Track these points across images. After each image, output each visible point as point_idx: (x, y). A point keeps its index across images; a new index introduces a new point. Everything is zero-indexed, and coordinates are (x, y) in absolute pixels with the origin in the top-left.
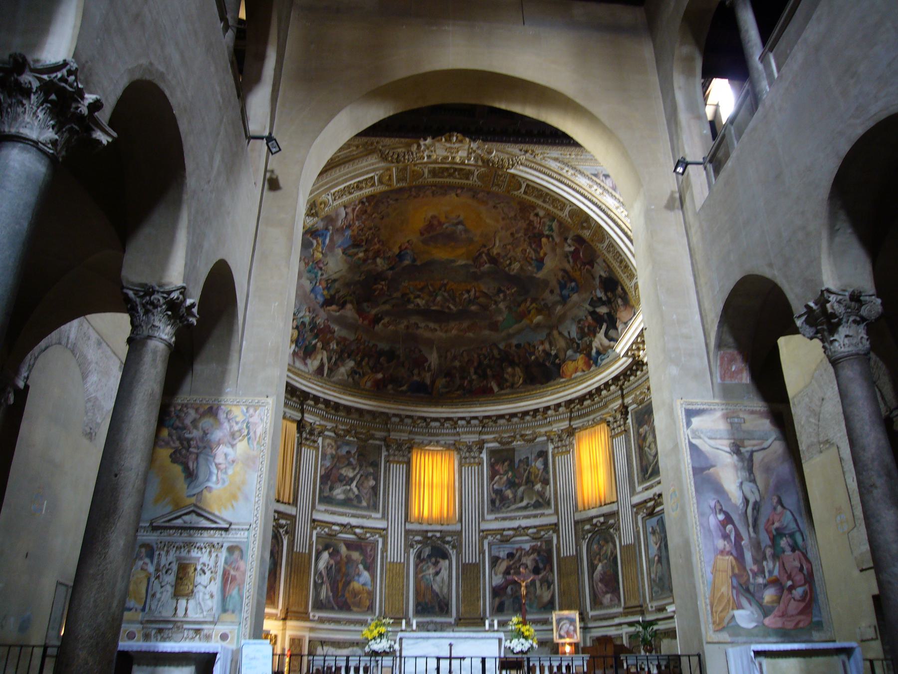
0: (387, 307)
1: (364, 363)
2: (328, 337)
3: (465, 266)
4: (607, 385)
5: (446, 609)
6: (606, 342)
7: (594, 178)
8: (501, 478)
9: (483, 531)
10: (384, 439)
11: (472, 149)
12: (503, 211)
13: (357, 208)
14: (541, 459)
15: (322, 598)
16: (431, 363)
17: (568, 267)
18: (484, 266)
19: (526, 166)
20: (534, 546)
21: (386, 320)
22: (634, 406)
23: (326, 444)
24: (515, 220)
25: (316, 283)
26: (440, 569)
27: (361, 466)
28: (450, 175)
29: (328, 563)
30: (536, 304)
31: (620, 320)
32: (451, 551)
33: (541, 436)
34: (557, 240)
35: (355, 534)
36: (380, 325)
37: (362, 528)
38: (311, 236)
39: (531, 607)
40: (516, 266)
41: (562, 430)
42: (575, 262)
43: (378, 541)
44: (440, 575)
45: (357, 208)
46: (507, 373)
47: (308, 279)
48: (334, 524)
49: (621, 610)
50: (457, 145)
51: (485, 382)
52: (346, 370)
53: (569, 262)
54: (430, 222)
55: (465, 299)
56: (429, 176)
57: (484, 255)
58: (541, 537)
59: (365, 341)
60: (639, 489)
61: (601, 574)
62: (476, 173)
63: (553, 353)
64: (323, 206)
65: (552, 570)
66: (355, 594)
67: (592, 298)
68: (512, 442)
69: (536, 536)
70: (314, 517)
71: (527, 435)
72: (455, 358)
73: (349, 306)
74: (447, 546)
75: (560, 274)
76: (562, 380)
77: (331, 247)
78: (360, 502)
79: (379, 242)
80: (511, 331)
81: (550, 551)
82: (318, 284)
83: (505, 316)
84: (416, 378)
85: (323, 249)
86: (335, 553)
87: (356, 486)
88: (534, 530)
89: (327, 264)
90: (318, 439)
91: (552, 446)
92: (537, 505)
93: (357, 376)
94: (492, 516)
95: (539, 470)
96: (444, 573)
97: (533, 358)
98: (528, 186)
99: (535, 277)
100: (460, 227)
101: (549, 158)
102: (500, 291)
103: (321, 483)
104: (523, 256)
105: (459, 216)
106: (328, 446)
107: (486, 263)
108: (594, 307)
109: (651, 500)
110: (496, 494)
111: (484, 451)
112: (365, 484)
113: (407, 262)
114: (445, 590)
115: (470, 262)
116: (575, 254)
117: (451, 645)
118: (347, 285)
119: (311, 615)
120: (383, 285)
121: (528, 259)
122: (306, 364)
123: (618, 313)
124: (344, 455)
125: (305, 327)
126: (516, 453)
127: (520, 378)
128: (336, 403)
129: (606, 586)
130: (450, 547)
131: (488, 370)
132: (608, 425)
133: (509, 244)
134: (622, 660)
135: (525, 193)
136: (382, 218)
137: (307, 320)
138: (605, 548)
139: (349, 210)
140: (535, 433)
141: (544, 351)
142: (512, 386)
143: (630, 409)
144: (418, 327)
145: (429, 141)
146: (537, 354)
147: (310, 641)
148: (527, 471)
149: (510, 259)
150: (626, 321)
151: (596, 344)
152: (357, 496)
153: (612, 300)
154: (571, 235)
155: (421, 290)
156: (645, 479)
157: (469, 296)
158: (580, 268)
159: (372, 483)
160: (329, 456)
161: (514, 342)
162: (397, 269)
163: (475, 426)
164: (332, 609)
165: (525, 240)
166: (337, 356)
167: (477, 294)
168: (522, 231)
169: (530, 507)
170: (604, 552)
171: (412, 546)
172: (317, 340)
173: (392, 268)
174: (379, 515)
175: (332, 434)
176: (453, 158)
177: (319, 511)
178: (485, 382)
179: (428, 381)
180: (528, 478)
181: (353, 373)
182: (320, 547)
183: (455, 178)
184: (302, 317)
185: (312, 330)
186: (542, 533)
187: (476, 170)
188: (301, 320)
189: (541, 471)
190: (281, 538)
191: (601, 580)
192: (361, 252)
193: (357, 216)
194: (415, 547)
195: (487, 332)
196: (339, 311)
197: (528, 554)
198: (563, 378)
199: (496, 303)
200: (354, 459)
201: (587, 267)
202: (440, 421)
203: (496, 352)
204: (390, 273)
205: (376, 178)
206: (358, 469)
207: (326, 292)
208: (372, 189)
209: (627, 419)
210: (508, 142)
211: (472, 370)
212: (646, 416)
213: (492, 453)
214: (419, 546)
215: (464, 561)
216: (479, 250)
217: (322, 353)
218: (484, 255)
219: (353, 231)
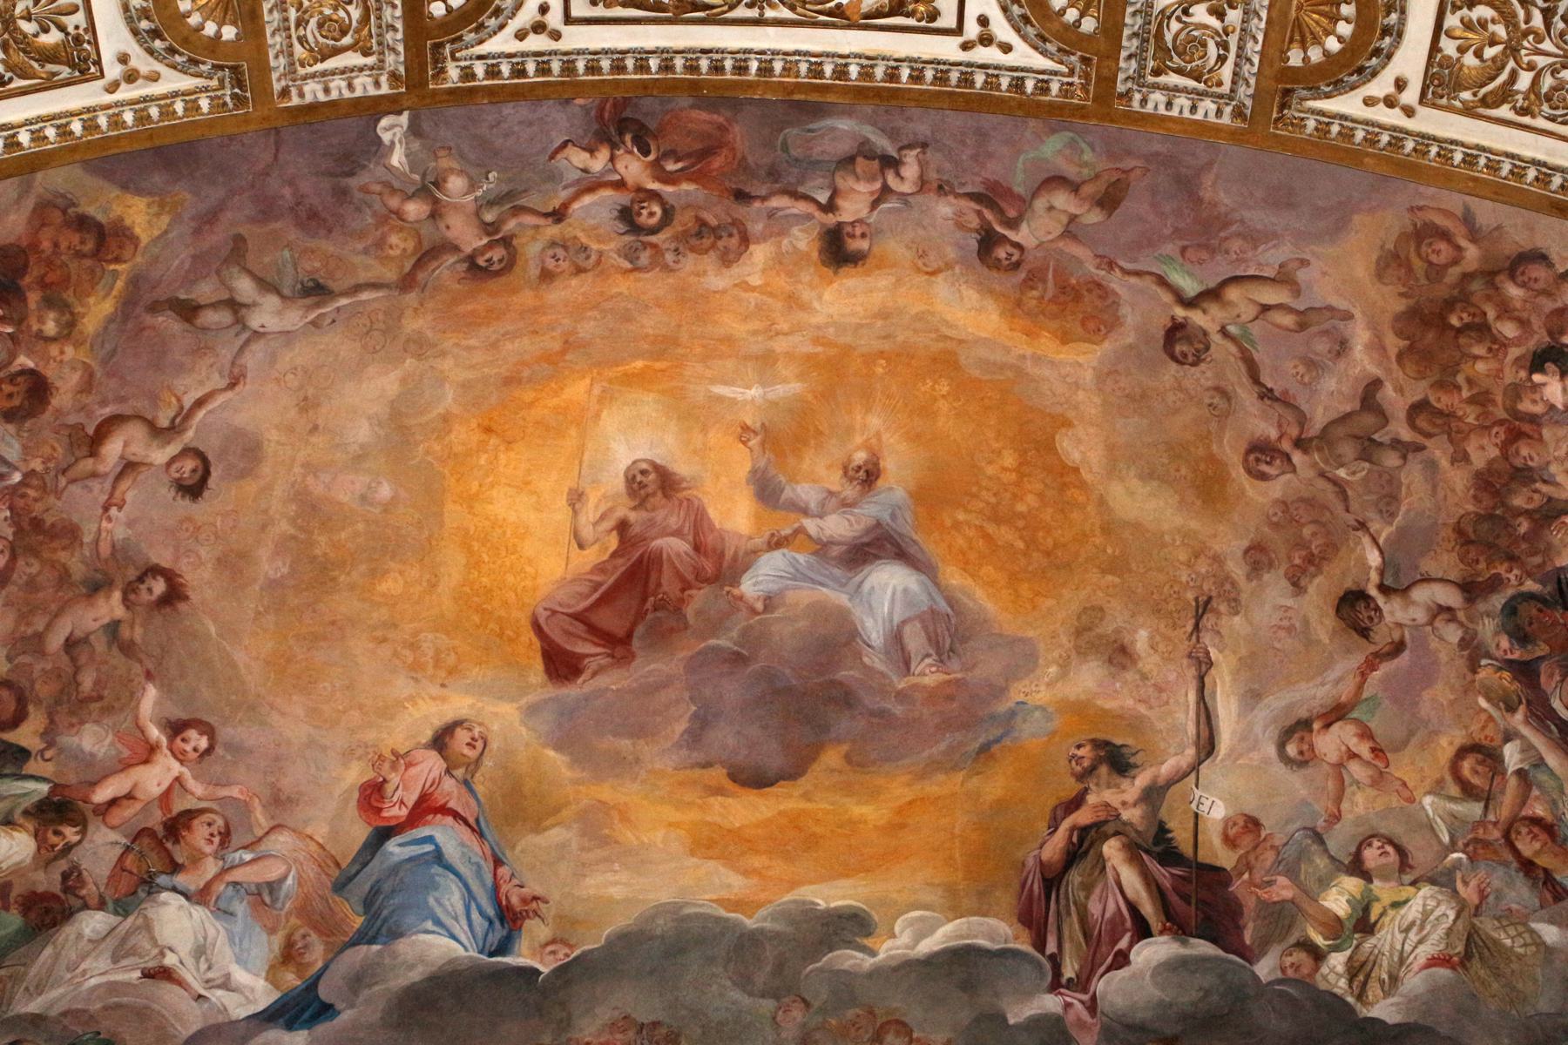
12: (1255, 378)
18: (1122, 960)
24: (1368, 448)
54: (622, 527)
57: (1112, 850)
79: (176, 729)
104: (1476, 809)
105: (869, 476)
107: (1143, 931)
121: (1527, 847)
133: (1336, 713)
136: (194, 489)
149: (1357, 867)
162: (346, 1016)
165: (1473, 651)
168: (1446, 562)
216: (1076, 803)
218: (1112, 850)
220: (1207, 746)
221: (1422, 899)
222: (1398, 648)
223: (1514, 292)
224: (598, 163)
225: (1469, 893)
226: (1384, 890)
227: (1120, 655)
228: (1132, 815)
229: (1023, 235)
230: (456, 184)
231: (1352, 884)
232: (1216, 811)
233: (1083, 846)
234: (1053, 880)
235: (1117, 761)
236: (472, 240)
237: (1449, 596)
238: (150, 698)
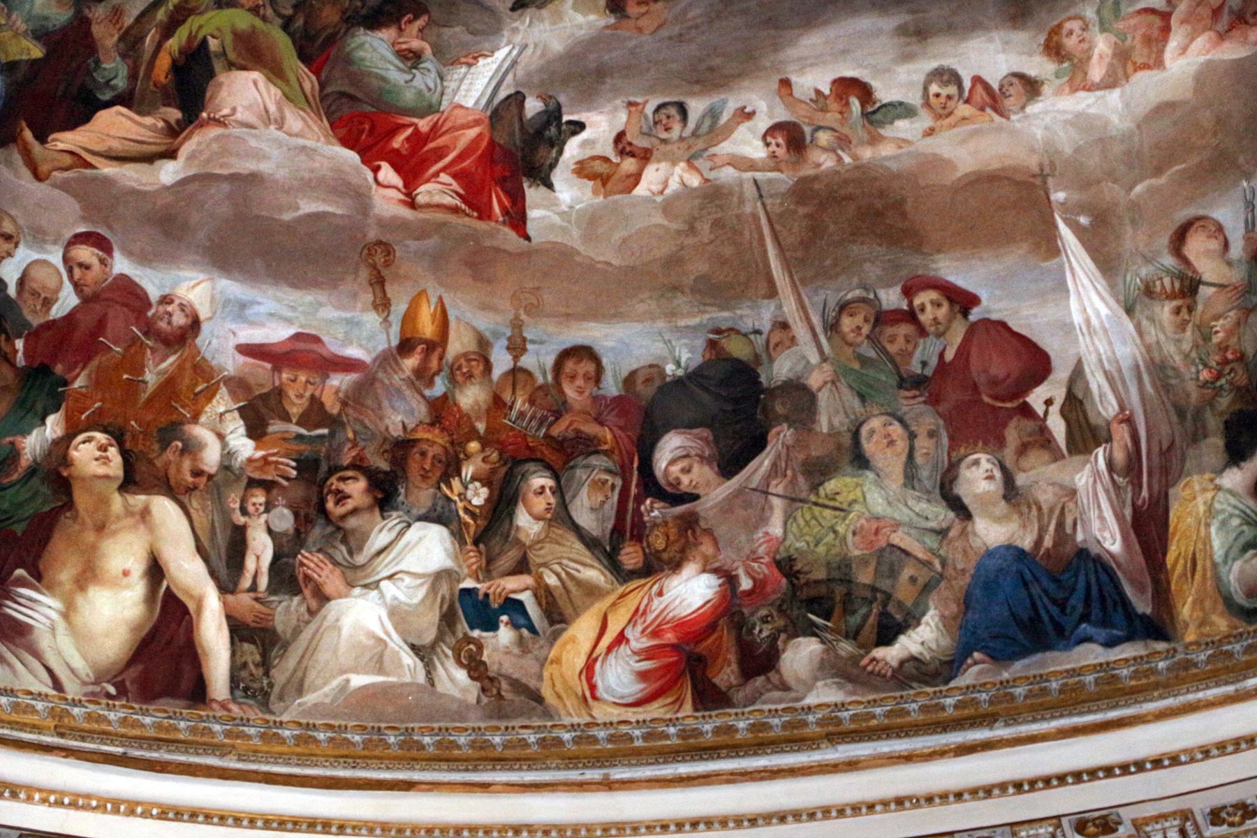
1: (526, 523)
2: (151, 377)
16: (1078, 373)
36: (560, 177)
52: (397, 614)
59: (483, 344)
166: (284, 519)
172: (53, 426)
196: (171, 154)
217: (145, 514)
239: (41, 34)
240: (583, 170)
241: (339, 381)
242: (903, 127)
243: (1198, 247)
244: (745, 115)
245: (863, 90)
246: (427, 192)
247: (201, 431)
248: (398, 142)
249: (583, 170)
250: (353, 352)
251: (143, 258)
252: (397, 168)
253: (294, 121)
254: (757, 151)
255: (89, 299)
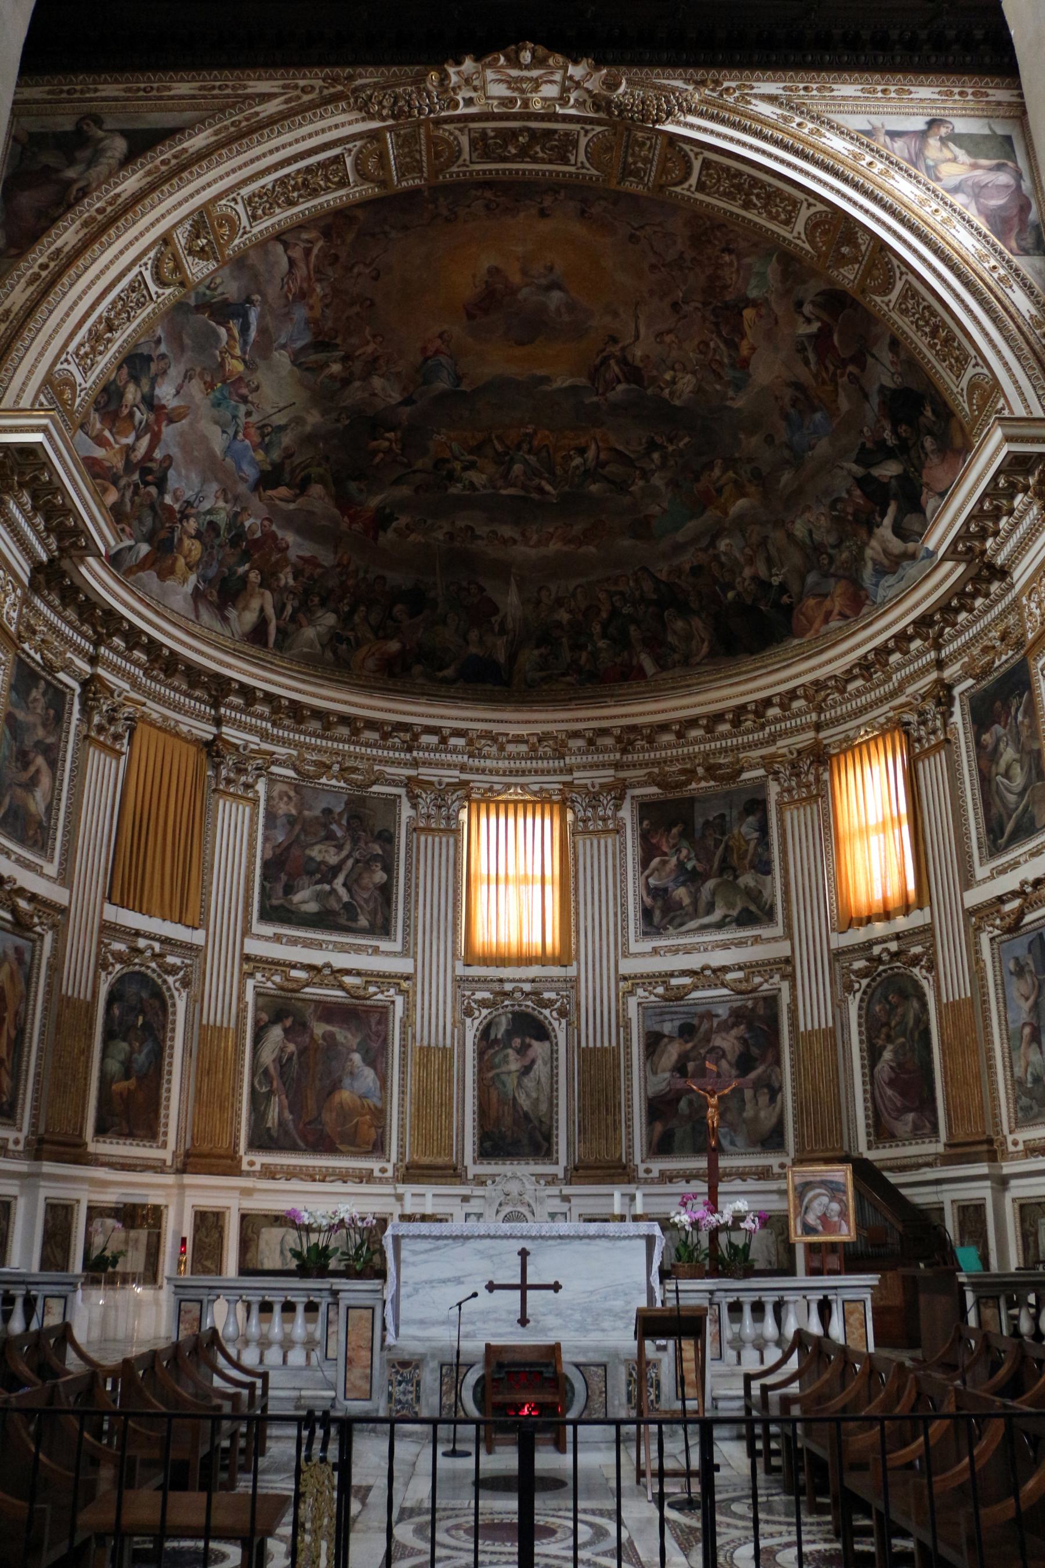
0: (405, 491)
1: (357, 619)
2: (273, 559)
3: (573, 388)
4: (902, 639)
5: (545, 1145)
6: (896, 545)
7: (865, 140)
8: (664, 863)
9: (625, 978)
10: (410, 783)
11: (571, 78)
13: (315, 251)
14: (751, 819)
15: (269, 1124)
16: (505, 616)
17: (804, 374)
18: (614, 389)
19: (701, 115)
20: (739, 1008)
21: (403, 520)
22: (970, 682)
23: (275, 794)
25: (236, 433)
26: (533, 1062)
27: (355, 841)
28: (524, 153)
29: (282, 1050)
30: (735, 473)
31: (931, 490)
32: (556, 1024)
33: (753, 767)
34: (779, 309)
35: (341, 987)
37: (358, 973)
38: (210, 316)
39: (733, 1143)
40: (687, 383)
41: (799, 752)
42: (821, 361)
43: (393, 1002)
44: (532, 1074)
45: (315, 251)
46: (675, 632)
47: (217, 423)
48: (294, 966)
49: (940, 1148)
50: (535, 73)
51: (626, 654)
52: (319, 635)
53: (807, 363)
55: (577, 467)
56: (475, 155)
57: (612, 362)
58: (754, 990)
60: (981, 872)
61: (891, 1067)
62: (583, 141)
63: (776, 581)
64: (225, 230)
65: (778, 1061)
66: (345, 1113)
67: (863, 444)
68: (688, 782)
69: (744, 986)
70: (246, 951)
71: (720, 766)
72: (559, 602)
73: (317, 489)
74: (546, 1012)
75: (789, 393)
76: (796, 642)
77: (265, 345)
78: (354, 918)
79: (374, 336)
80: (680, 537)
81: (773, 1021)
82: (240, 436)
83: (665, 505)
84: (473, 650)
85: (244, 352)
86: (298, 1029)
87: (345, 885)
88: (740, 975)
89: (257, 388)
90: (256, 782)
91: (778, 789)
92: (746, 919)
93: (344, 646)
94: (647, 945)
95: (747, 842)
96: (540, 1069)
97: (730, 595)
98: (706, 164)
99: (730, 408)
100: (556, 295)
101: (756, 96)
102: (652, 446)
103: (265, 877)
105: (551, 269)
106: (281, 799)
107: (619, 382)
108: (868, 465)
109: (1014, 894)
110: (654, 898)
111: (627, 805)
112: (365, 881)
113: (443, 384)
114: (544, 1107)
115: (583, 381)
116: (821, 341)
117: (524, 1254)
118: (308, 440)
119: (245, 1160)
120: (388, 440)
121: (714, 367)
122: (225, 619)
123: (925, 472)
124: (317, 818)
125: (218, 535)
126: (697, 806)
127: (703, 641)
128: (292, 701)
129: (903, 1094)
130: (555, 1014)
131: (632, 628)
132: (907, 733)
134: (963, 1284)
135: (701, 187)
136: (376, 278)
137: (221, 519)
138: (900, 1010)
139: (297, 253)
140: (738, 761)
141: (755, 578)
142: (686, 662)
143: (956, 691)
144: (475, 537)
145: (468, 65)
146: (740, 588)
147: (243, 1217)
148: (722, 846)
149: (673, 369)
150: (940, 488)
151: (873, 550)
152: (347, 906)
153: (910, 443)
154: (813, 287)
155: (478, 450)
156: (998, 850)
157: (585, 461)
158: (834, 374)
159: (380, 877)
160: (284, 820)
161: (687, 560)
163: (606, 750)
164: (293, 1148)
165: (704, 318)
166: (296, 603)
167: (603, 456)
169: (730, 923)
170: (897, 1018)
171: (468, 1012)
172: (247, 567)
173: (408, 401)
174: (397, 947)
175: (291, 773)
176: (526, 103)
177: (259, 937)
178: (626, 654)
179: (501, 657)
180: (724, 860)
181: (334, 638)
182: (265, 1017)
183: (535, 160)
184: (209, 512)
185: (234, 542)
186: (758, 980)
187: (582, 132)
188: (208, 518)
189: (752, 844)
190: (172, 997)
191: (891, 1083)
192: (335, 362)
193: (318, 271)
194: (477, 1013)
195: (626, 543)
197: (725, 1027)
198: (801, 635)
199: (645, 475)
200: (340, 825)
201: (851, 368)
202: (526, 742)
203: (647, 586)
204: (408, 409)
205: (349, 161)
206: (348, 847)
207: (260, 456)
208: (342, 192)
209: (951, 714)
210: (652, 64)
211: (597, 629)
212: (998, 704)
213: (646, 809)
214: (485, 1012)
215: (583, 1044)
217: (263, 594)
218: (612, 362)
219: (312, 308)
220: (637, 337)
221: (689, 377)
222: (685, 317)
223: (718, 234)
224: (479, 193)
225: (699, 376)
226: (680, 375)
227: (615, 314)
228: (618, 354)
229: (593, 210)
230: (441, 199)
231: (672, 373)
232: (639, 353)
233: (605, 361)
234: (597, 369)
235: (614, 340)
236: (445, 212)
237: (699, 305)
238: (368, 330)
239: (272, 464)
240: (395, 530)
241: (319, 570)
242: (480, 542)
243: (544, 593)
244: (441, 527)
245: (472, 529)
246: (354, 526)
247: (282, 576)
248: (351, 511)
249: (395, 530)
250: (326, 564)
251: (279, 527)
252: (350, 517)
253: (326, 500)
254: (441, 538)
255: (264, 534)
